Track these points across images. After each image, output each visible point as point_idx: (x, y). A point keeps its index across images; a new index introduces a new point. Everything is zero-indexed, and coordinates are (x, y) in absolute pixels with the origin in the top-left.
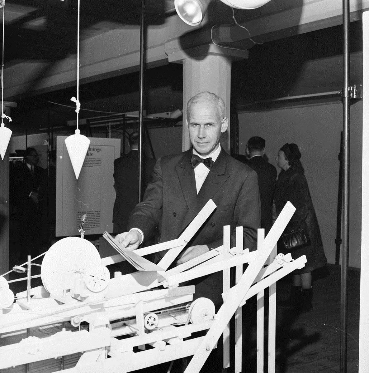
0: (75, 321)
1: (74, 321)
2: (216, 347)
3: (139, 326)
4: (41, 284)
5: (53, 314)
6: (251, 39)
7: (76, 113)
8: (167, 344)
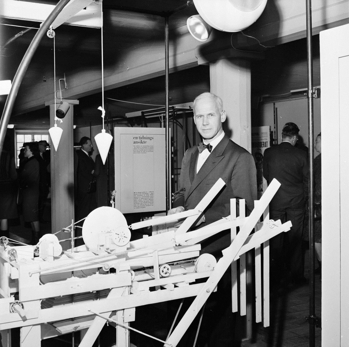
0: (105, 267)
1: (105, 267)
2: (216, 290)
3: (156, 273)
4: (83, 243)
5: (88, 261)
6: (261, 45)
7: (102, 118)
8: (175, 286)
